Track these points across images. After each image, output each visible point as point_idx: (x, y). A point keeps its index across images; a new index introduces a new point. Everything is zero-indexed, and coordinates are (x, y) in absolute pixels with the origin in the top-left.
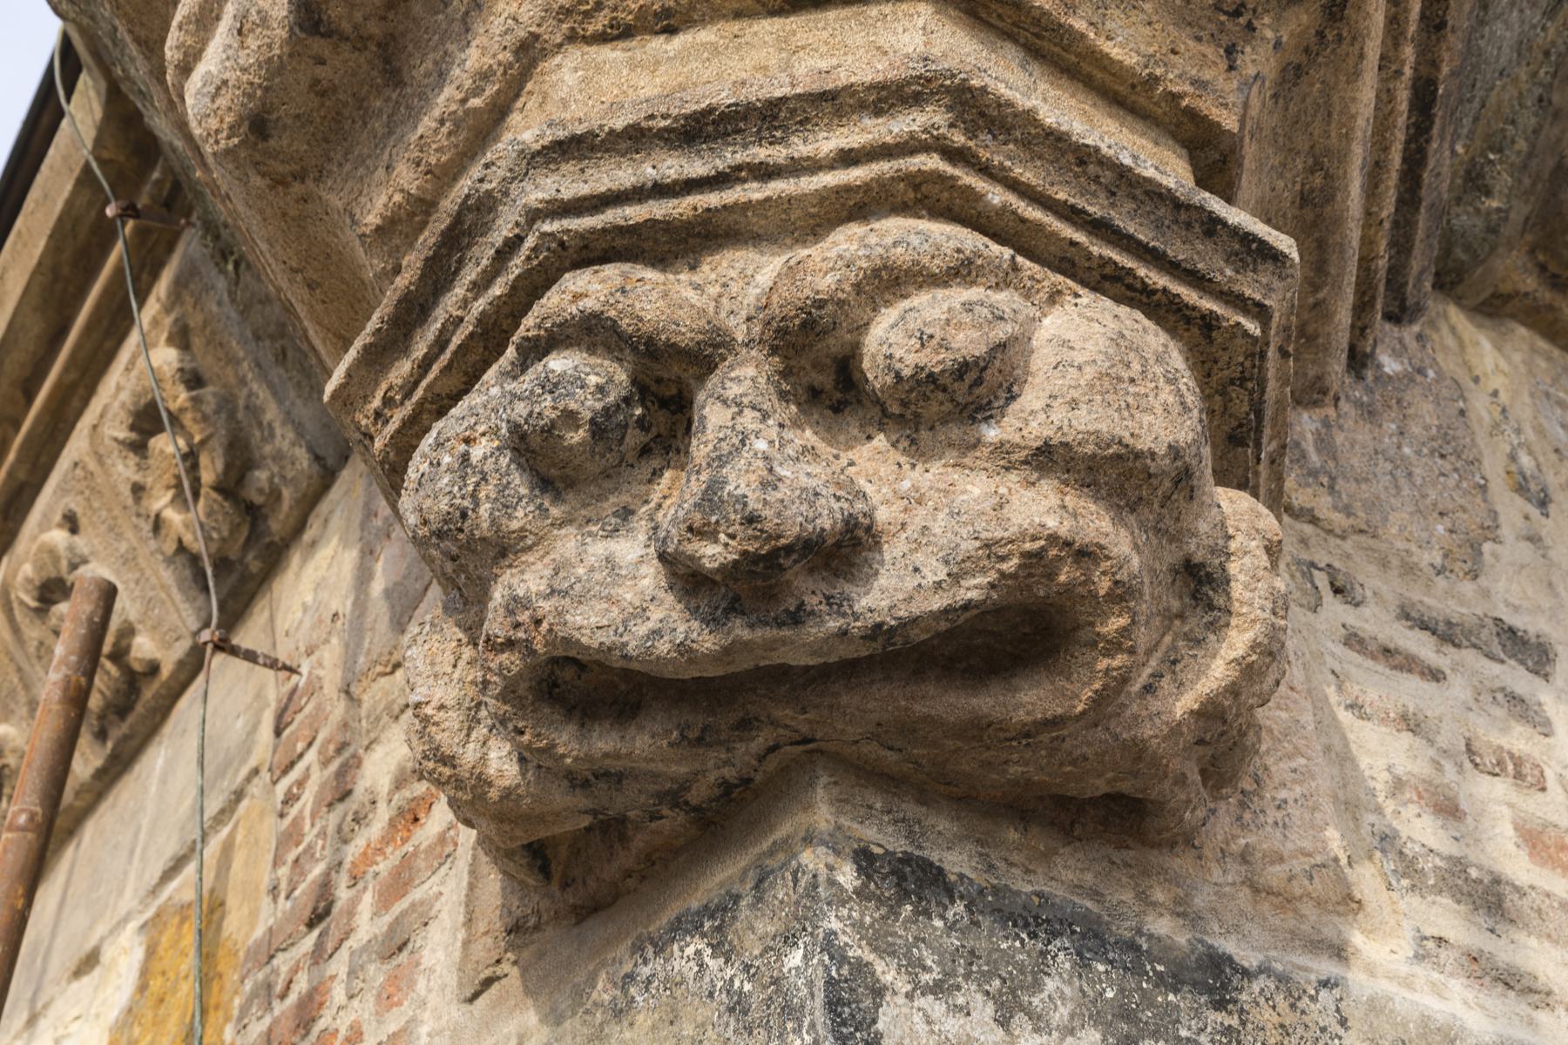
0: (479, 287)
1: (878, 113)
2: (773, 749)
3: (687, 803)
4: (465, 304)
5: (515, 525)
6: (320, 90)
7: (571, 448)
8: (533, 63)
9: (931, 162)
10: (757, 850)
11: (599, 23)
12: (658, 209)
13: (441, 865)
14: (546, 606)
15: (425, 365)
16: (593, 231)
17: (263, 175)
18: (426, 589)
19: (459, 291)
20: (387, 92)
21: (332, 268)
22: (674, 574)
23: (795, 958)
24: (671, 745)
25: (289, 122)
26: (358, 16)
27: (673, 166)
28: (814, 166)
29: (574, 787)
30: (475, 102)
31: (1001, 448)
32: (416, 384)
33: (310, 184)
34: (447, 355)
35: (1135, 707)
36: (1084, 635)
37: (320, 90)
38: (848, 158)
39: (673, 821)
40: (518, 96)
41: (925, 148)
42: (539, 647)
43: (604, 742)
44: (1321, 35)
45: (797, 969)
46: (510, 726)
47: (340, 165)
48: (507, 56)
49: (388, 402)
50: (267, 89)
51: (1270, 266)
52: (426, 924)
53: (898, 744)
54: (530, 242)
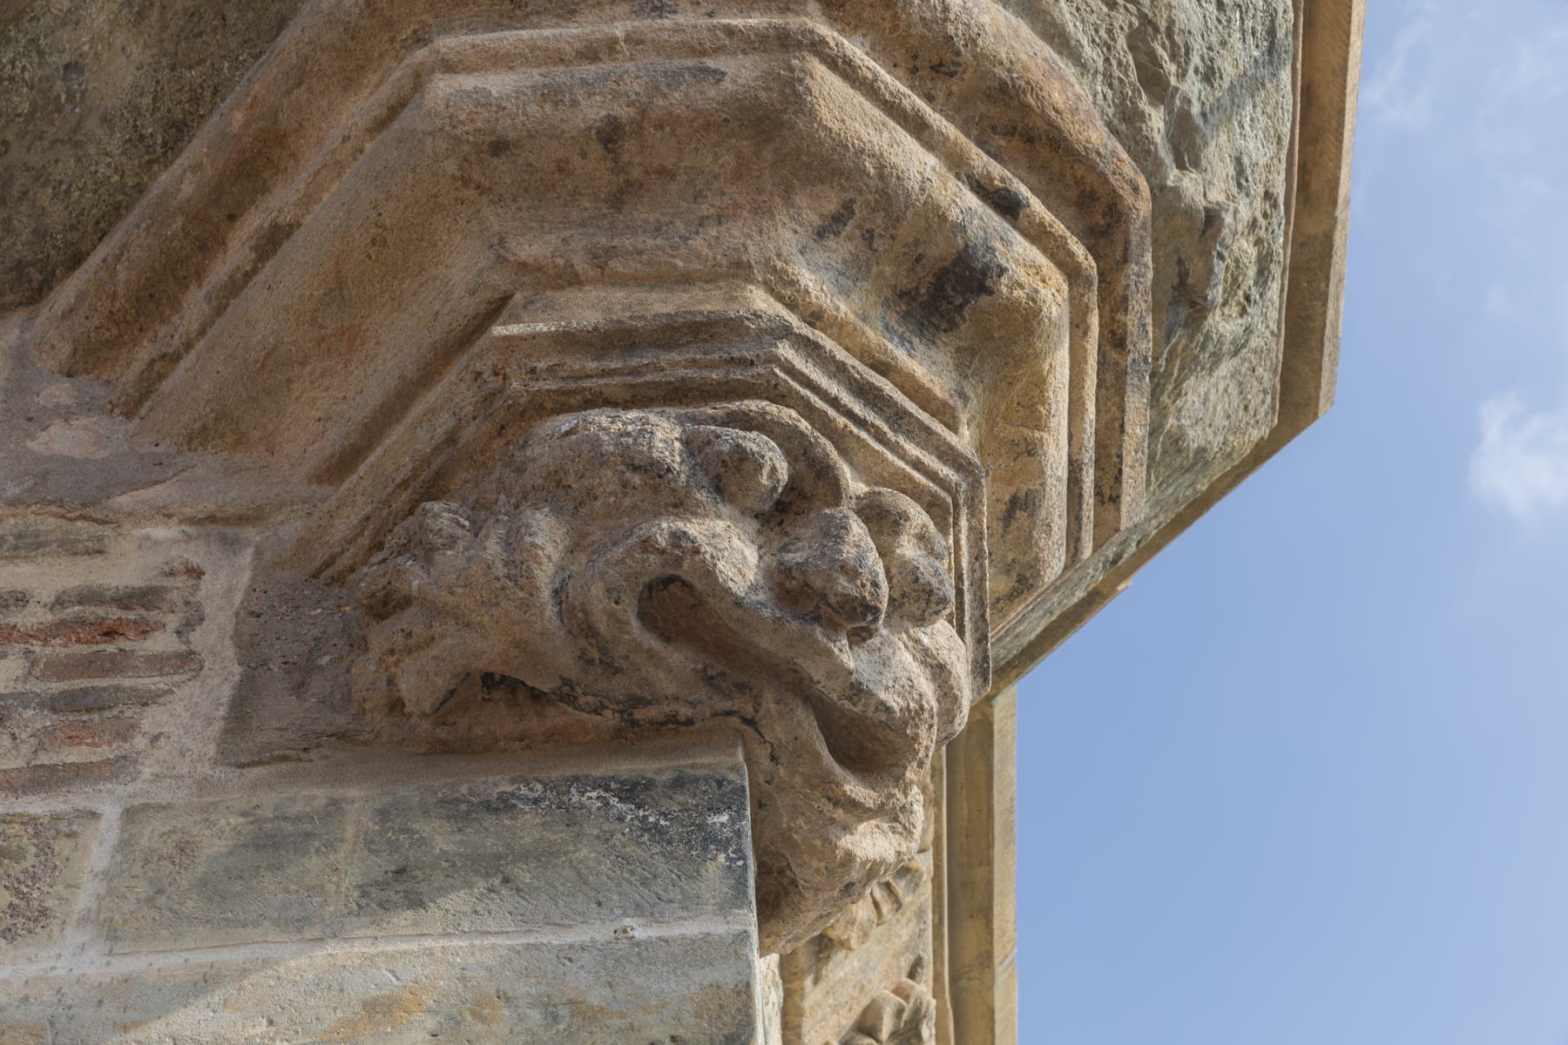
0: (694, 363)
1: (940, 457)
2: (729, 713)
3: (631, 714)
4: (675, 364)
5: (698, 496)
6: (562, 167)
7: (759, 484)
8: (735, 276)
9: (949, 500)
10: (675, 762)
11: (787, 292)
12: (831, 412)
13: (175, 673)
14: (706, 548)
15: (605, 373)
16: (797, 393)
17: (461, 168)
18: (156, 483)
19: (675, 356)
20: (602, 205)
21: (412, 247)
22: (780, 585)
23: (724, 818)
24: (694, 669)
25: (521, 161)
26: (637, 160)
27: (846, 398)
28: (902, 455)
29: (580, 658)
30: (680, 264)
31: (926, 652)
32: (588, 377)
33: (484, 199)
34: (639, 380)
35: (857, 837)
36: (896, 770)
37: (562, 167)
38: (917, 464)
39: (610, 719)
40: (707, 282)
41: (949, 491)
42: (685, 566)
43: (651, 642)
44: (998, 600)
45: (722, 824)
46: (615, 595)
47: (520, 209)
48: (725, 262)
49: (551, 370)
50: (531, 136)
51: (980, 680)
52: (146, 704)
53: (783, 759)
54: (760, 370)
